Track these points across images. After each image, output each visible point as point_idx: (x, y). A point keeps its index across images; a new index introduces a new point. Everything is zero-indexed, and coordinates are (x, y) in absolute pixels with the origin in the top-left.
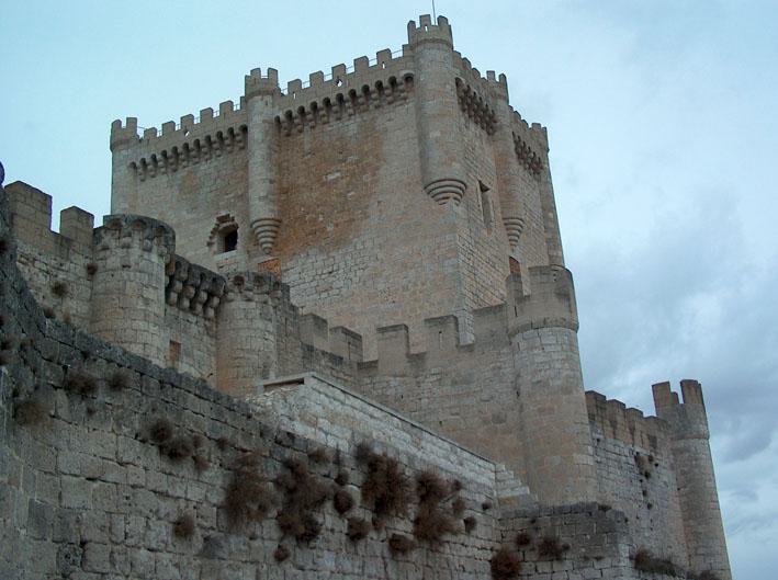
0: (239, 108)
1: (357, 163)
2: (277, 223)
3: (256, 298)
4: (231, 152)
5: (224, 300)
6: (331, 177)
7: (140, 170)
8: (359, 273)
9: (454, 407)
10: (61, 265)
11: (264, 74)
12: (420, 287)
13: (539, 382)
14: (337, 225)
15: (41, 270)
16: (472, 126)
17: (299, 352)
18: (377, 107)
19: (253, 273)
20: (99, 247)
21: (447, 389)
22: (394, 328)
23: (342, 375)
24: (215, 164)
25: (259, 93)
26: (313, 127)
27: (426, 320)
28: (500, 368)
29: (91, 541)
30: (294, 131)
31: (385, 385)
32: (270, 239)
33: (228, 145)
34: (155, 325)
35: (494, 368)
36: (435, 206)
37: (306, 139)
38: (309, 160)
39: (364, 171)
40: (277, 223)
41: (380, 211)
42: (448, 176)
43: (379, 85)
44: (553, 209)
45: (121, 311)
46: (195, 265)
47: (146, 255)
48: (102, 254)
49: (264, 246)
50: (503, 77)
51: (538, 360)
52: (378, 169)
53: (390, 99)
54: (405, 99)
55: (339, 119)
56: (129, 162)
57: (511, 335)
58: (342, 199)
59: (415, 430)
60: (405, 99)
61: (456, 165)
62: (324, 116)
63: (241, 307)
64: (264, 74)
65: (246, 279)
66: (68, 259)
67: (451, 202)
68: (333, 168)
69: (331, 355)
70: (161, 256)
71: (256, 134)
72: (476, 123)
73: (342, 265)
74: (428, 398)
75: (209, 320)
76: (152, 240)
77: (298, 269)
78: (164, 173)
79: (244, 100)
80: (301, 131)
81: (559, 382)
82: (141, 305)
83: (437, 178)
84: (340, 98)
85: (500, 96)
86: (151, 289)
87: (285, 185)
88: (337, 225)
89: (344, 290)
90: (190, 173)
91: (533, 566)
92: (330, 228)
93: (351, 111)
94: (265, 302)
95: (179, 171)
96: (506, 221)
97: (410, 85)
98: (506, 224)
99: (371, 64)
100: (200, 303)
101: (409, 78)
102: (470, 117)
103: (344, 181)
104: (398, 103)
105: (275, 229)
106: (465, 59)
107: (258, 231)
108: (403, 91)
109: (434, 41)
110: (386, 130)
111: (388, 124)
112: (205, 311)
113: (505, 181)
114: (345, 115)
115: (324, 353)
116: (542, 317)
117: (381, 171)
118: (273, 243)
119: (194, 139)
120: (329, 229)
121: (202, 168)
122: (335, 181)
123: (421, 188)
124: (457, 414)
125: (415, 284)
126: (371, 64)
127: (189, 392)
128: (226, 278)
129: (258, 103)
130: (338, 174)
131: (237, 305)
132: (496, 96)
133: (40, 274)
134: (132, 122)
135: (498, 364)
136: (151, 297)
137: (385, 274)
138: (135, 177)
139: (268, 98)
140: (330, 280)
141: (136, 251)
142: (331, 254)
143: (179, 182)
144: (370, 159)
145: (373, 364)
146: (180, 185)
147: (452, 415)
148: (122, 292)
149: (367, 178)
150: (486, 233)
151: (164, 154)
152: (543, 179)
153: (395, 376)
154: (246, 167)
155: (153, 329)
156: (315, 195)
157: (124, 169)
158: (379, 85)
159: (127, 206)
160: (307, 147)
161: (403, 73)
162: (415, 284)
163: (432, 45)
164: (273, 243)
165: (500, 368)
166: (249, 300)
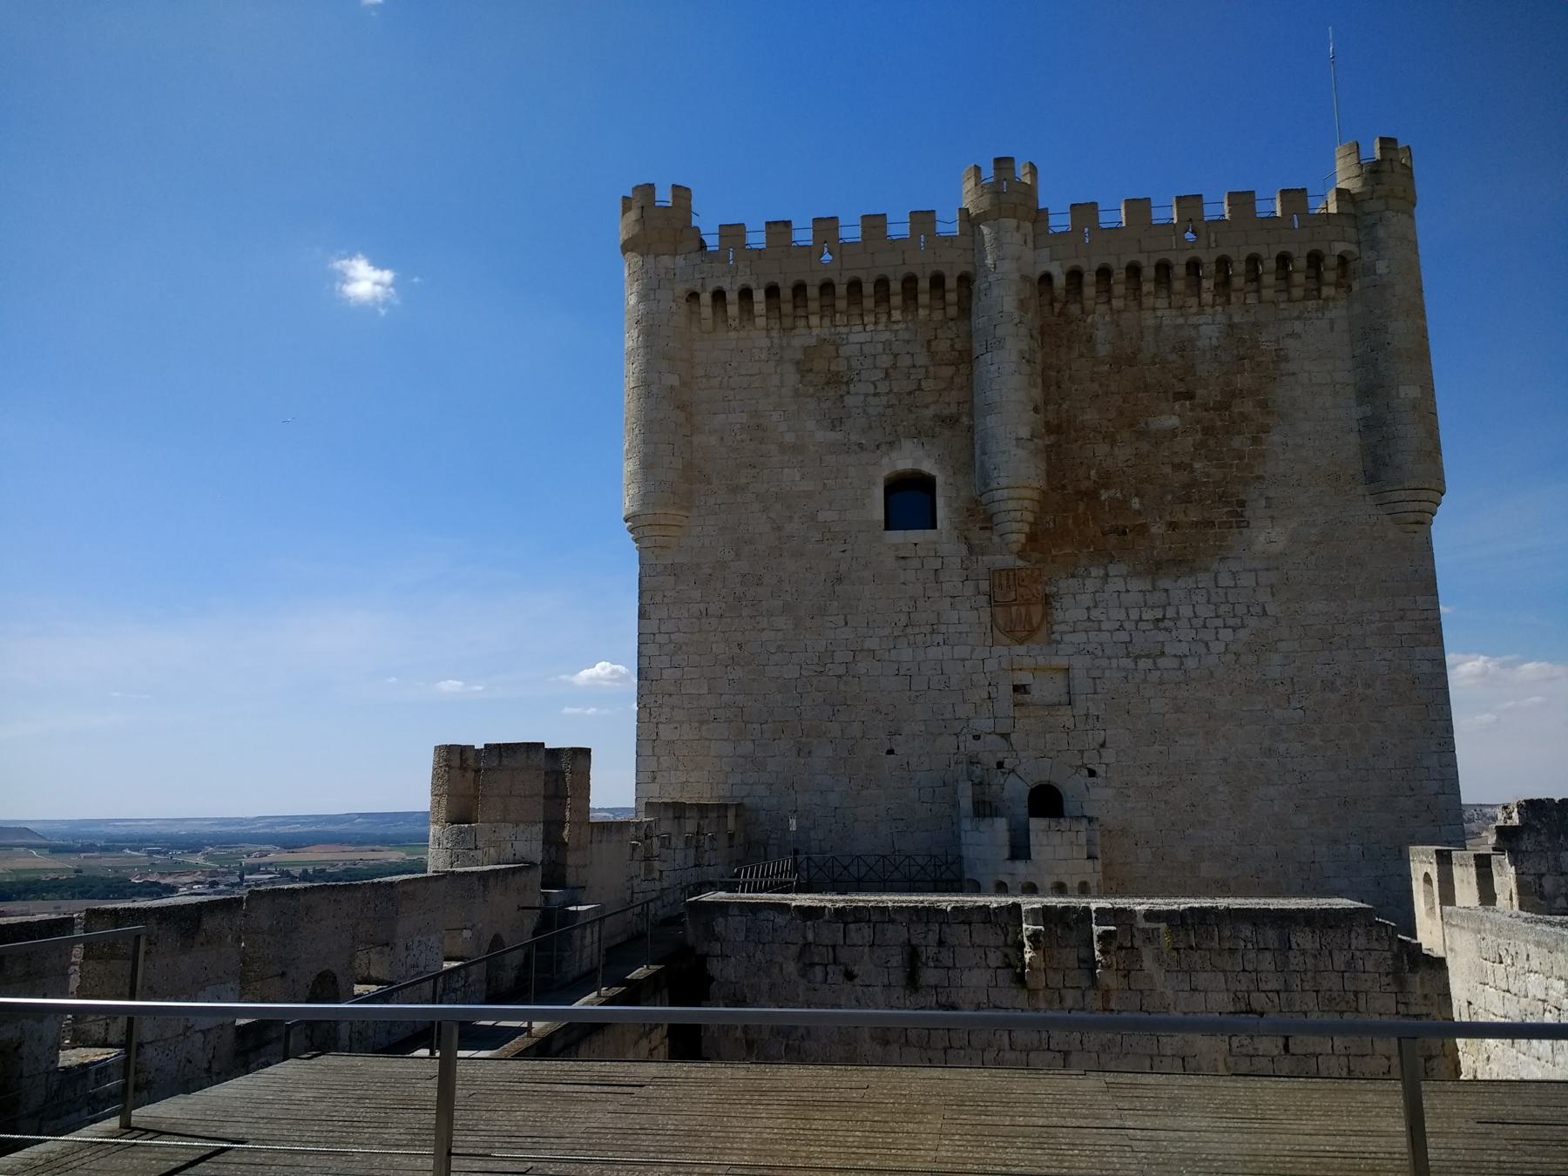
0: (955, 229)
8: (1226, 635)
14: (1173, 526)
24: (887, 336)
33: (924, 307)
52: (1265, 429)
54: (1327, 299)
58: (1183, 477)
73: (1186, 611)
84: (1194, 266)
88: (1173, 526)
93: (1207, 297)
95: (797, 331)
120: (1154, 530)
121: (853, 338)
122: (1173, 433)
137: (1283, 646)
140: (1161, 636)
142: (1165, 583)
143: (799, 356)
154: (965, 359)
159: (676, 383)
160: (1103, 350)
161: (1339, 248)
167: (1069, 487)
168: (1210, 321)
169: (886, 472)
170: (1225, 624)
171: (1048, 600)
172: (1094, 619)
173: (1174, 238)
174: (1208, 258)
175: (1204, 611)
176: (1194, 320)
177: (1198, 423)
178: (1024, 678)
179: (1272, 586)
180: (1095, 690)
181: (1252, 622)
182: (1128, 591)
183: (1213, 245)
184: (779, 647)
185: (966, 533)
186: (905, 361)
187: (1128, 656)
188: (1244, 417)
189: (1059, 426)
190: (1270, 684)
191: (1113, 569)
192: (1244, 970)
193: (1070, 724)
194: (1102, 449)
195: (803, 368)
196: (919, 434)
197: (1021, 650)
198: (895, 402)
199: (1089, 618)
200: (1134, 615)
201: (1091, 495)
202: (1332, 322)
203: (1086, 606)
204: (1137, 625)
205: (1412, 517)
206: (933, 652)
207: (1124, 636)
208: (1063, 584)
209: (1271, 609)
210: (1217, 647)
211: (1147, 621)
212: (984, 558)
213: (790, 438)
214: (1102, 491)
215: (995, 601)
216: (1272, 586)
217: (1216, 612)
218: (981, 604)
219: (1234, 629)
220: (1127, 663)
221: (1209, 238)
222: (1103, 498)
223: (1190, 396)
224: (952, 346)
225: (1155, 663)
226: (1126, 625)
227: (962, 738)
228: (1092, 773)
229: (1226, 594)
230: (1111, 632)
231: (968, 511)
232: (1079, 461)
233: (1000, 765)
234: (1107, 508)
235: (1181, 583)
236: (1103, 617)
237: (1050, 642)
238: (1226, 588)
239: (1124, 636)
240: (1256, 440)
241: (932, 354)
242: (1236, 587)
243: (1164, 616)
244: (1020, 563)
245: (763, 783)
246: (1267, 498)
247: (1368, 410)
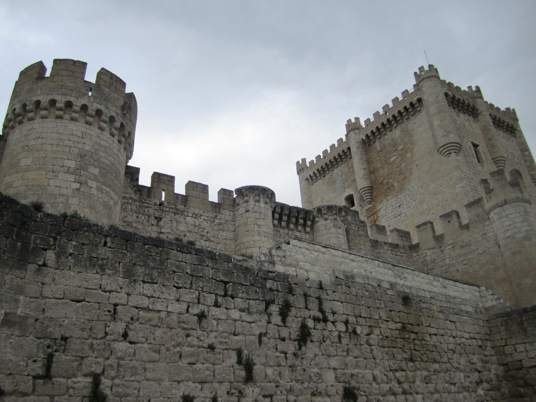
1: (403, 149)
2: (371, 188)
3: (330, 218)
4: (346, 161)
5: (313, 222)
6: (392, 160)
7: (310, 180)
8: (414, 203)
9: (464, 260)
10: (216, 216)
11: (353, 121)
13: (508, 237)
14: (398, 182)
15: (204, 220)
16: (462, 115)
17: (368, 244)
18: (407, 119)
19: (326, 206)
20: (236, 205)
21: (458, 251)
22: (424, 224)
23: (399, 253)
25: (352, 130)
26: (379, 139)
27: (441, 216)
28: (486, 234)
29: (71, 337)
30: (372, 143)
31: (424, 255)
32: (369, 197)
34: (265, 237)
35: (482, 235)
36: (445, 159)
37: (377, 145)
39: (407, 152)
40: (371, 188)
41: (418, 169)
42: (448, 142)
43: (405, 108)
44: (527, 149)
45: (246, 233)
46: (293, 207)
47: (257, 204)
48: (237, 208)
49: (367, 200)
50: (477, 87)
51: (506, 223)
53: (412, 113)
55: (391, 131)
56: (305, 178)
57: (488, 213)
59: (396, 268)
60: (420, 111)
61: (452, 135)
62: (383, 131)
63: (323, 224)
64: (353, 121)
65: (323, 209)
66: (220, 213)
67: (453, 155)
68: (392, 155)
69: (391, 244)
70: (266, 203)
71: (353, 149)
72: (464, 113)
73: (405, 201)
74: (449, 258)
75: (308, 233)
76: (259, 196)
77: (384, 208)
78: (320, 179)
79: (347, 136)
80: (374, 142)
81: (522, 235)
82: (256, 228)
83: (442, 145)
84: (388, 120)
85: (477, 97)
86: (261, 220)
87: (371, 169)
89: (407, 213)
90: (330, 176)
91: (513, 348)
92: (396, 184)
93: (395, 125)
94: (335, 219)
96: (494, 160)
97: (421, 103)
98: (494, 162)
99: (400, 100)
100: (300, 225)
101: (420, 100)
102: (459, 111)
103: (398, 160)
104: (417, 114)
105: (370, 191)
106: (449, 83)
108: (418, 107)
109: (428, 77)
112: (305, 229)
113: (489, 140)
114: (393, 128)
115: (385, 243)
116: (503, 199)
117: (415, 151)
118: (370, 198)
119: (329, 160)
123: (436, 152)
124: (466, 264)
126: (400, 100)
127: (173, 250)
128: (313, 211)
129: (352, 135)
130: (395, 157)
131: (321, 223)
132: (475, 98)
133: (204, 222)
134: (304, 160)
135: (484, 232)
136: (261, 224)
138: (309, 184)
139: (357, 131)
140: (400, 209)
141: (252, 202)
142: (399, 196)
145: (417, 246)
146: (327, 183)
147: (464, 265)
148: (246, 224)
149: (409, 155)
150: (480, 168)
152: (518, 135)
153: (429, 249)
155: (263, 239)
156: (386, 170)
157: (303, 182)
158: (405, 108)
160: (378, 149)
161: (415, 99)
163: (427, 80)
164: (370, 198)
165: (486, 234)
166: (326, 219)
169: (344, 198)
174: (391, 118)
175: (408, 199)
176: (394, 132)
186: (344, 172)
188: (408, 148)
189: (373, 171)
191: (389, 198)
196: (348, 187)
201: (382, 182)
202: (422, 115)
205: (446, 153)
207: (393, 213)
209: (422, 192)
210: (412, 207)
219: (415, 200)
223: (396, 150)
226: (394, 210)
235: (402, 195)
239: (393, 213)
240: (412, 152)
241: (348, 168)
244: (371, 206)
246: (417, 165)
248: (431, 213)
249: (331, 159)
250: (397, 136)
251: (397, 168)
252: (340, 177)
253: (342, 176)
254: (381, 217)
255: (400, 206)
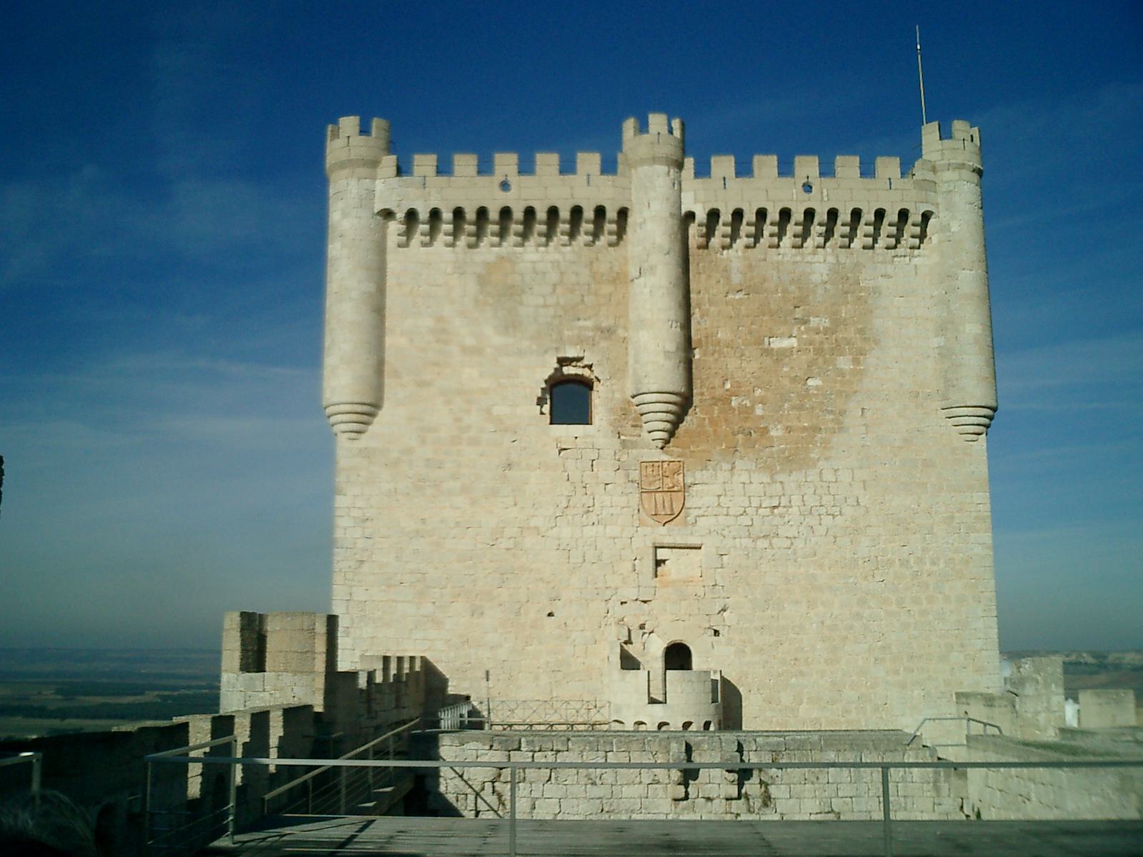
1: (826, 330)
8: (827, 521)
12: (928, 566)
14: (789, 430)
24: (557, 256)
38: (740, 301)
39: (837, 349)
68: (783, 329)
73: (796, 500)
89: (799, 544)
92: (776, 432)
107: (645, 408)
110: (876, 291)
111: (882, 282)
117: (871, 360)
120: (773, 433)
125: (920, 561)
130: (793, 342)
140: (777, 521)
142: (780, 477)
144: (851, 333)
149: (844, 363)
151: (458, 213)
154: (620, 279)
160: (736, 279)
162: (920, 561)
167: (706, 394)
168: (822, 260)
170: (827, 512)
171: (685, 488)
172: (723, 506)
173: (794, 190)
176: (809, 258)
177: (810, 344)
178: (662, 554)
179: (864, 482)
180: (722, 564)
181: (848, 511)
182: (751, 482)
183: (826, 199)
184: (458, 523)
185: (619, 429)
187: (749, 537)
190: (861, 562)
192: (828, 783)
193: (701, 593)
194: (733, 363)
195: (482, 280)
197: (663, 530)
198: (561, 312)
199: (719, 504)
200: (755, 503)
201: (726, 400)
203: (717, 494)
204: (757, 511)
206: (590, 531)
208: (699, 476)
210: (820, 530)
211: (766, 508)
212: (633, 451)
213: (470, 341)
214: (734, 398)
215: (642, 489)
216: (864, 482)
217: (821, 503)
218: (630, 491)
220: (746, 542)
221: (822, 193)
222: (733, 404)
223: (805, 322)
224: (611, 268)
225: (771, 544)
227: (611, 603)
228: (716, 633)
229: (829, 487)
230: (737, 517)
231: (622, 410)
232: (715, 371)
233: (642, 627)
234: (737, 412)
235: (794, 476)
236: (730, 504)
237: (685, 524)
238: (829, 483)
241: (594, 275)
242: (836, 481)
243: (779, 504)
244: (665, 458)
245: (442, 639)
246: (863, 409)
247: (940, 341)
248: (878, 578)
249: (536, 205)
250: (816, 278)
251: (794, 380)
252: (549, 289)
253: (555, 286)
254: (696, 512)
255: (774, 507)
